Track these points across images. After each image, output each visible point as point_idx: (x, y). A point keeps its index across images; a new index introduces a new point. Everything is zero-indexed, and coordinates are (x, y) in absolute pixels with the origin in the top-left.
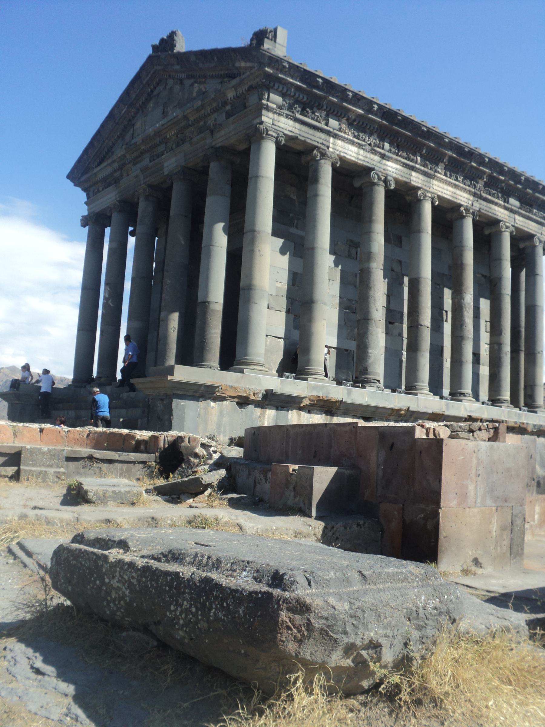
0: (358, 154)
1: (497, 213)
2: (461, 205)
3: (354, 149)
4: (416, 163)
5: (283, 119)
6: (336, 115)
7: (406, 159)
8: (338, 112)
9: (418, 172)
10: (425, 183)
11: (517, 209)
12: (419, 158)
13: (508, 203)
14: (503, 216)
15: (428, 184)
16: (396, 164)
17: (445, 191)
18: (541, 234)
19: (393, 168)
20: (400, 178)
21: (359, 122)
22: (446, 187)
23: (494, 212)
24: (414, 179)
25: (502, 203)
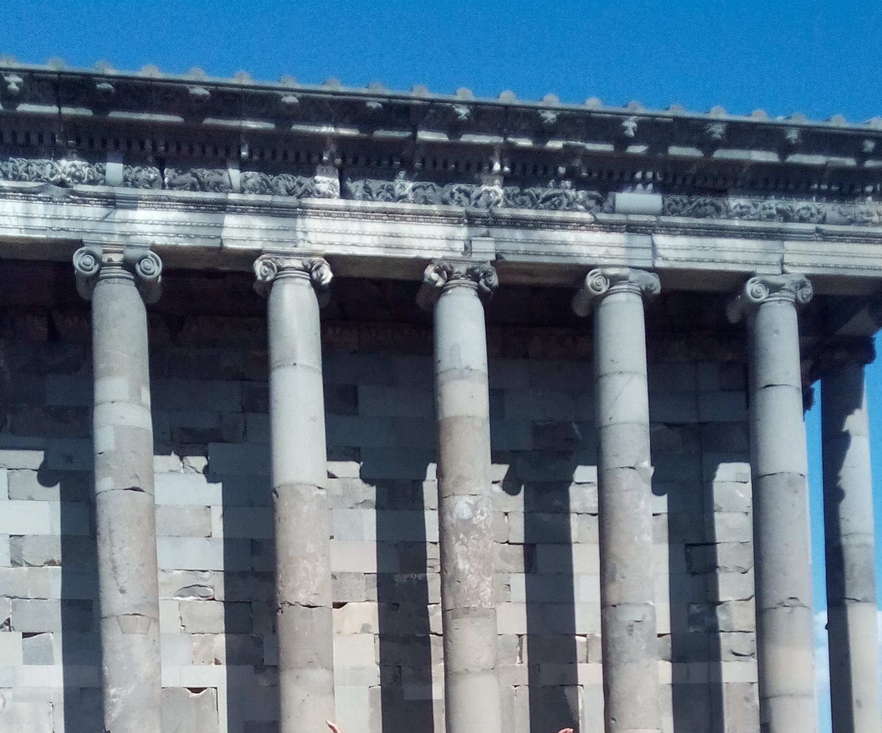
0: (28, 217)
1: (576, 249)
7: (193, 188)
9: (242, 212)
10: (274, 236)
11: (653, 219)
13: (613, 210)
14: (602, 251)
15: (286, 236)
16: (163, 207)
17: (355, 239)
18: (782, 263)
19: (156, 223)
20: (184, 243)
22: (354, 226)
23: (562, 249)
24: (236, 234)
25: (587, 216)
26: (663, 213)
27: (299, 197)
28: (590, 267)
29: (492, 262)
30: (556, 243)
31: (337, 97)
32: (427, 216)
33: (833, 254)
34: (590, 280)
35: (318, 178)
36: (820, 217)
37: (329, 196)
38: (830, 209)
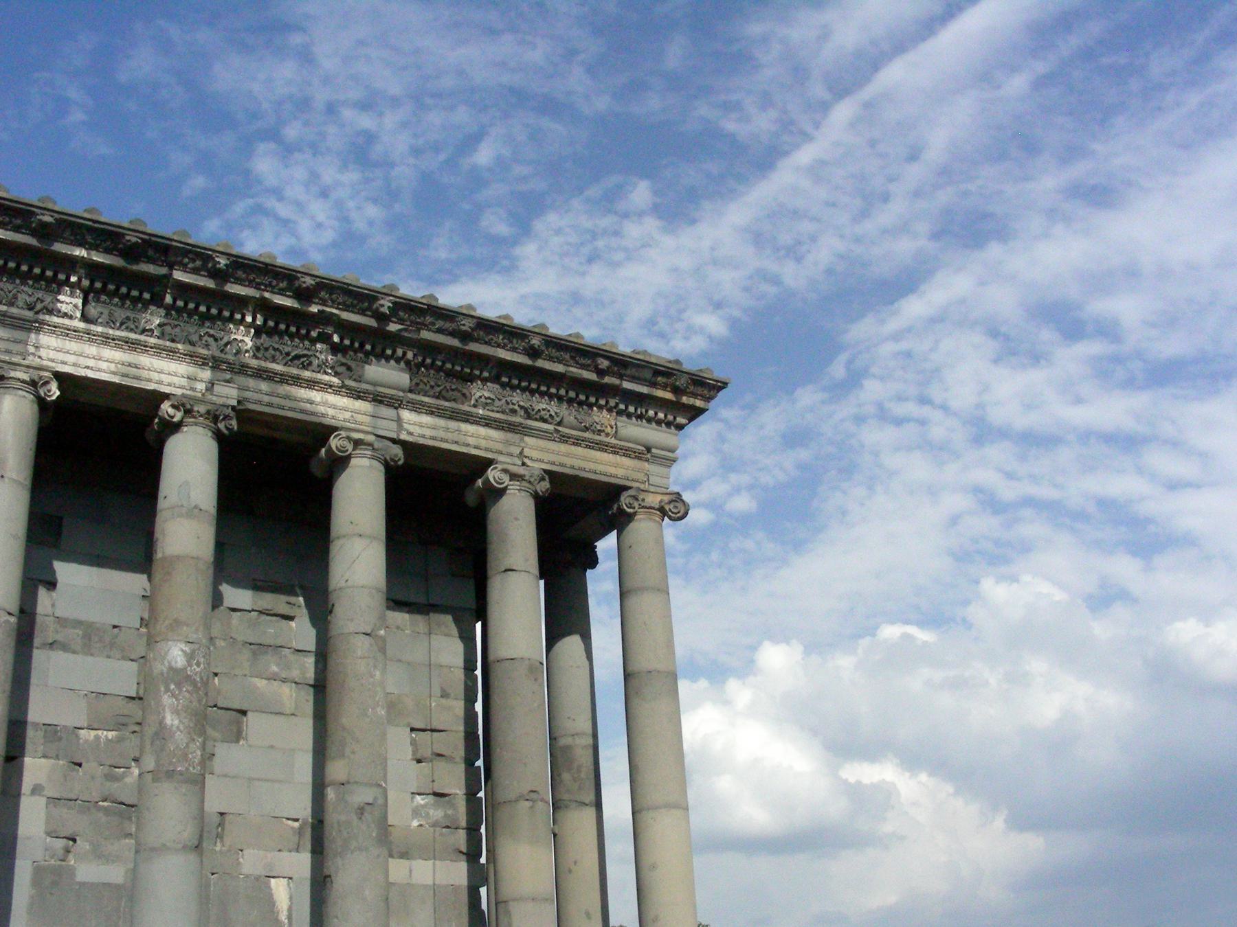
1: (321, 409)
2: (167, 396)
11: (401, 394)
14: (347, 415)
15: (15, 348)
17: (91, 363)
22: (92, 350)
25: (336, 380)
26: (411, 391)
27: (37, 313)
28: (335, 429)
29: (233, 408)
30: (301, 400)
31: (96, 225)
32: (172, 354)
33: (568, 455)
34: (334, 443)
35: (61, 297)
36: (558, 419)
37: (65, 315)
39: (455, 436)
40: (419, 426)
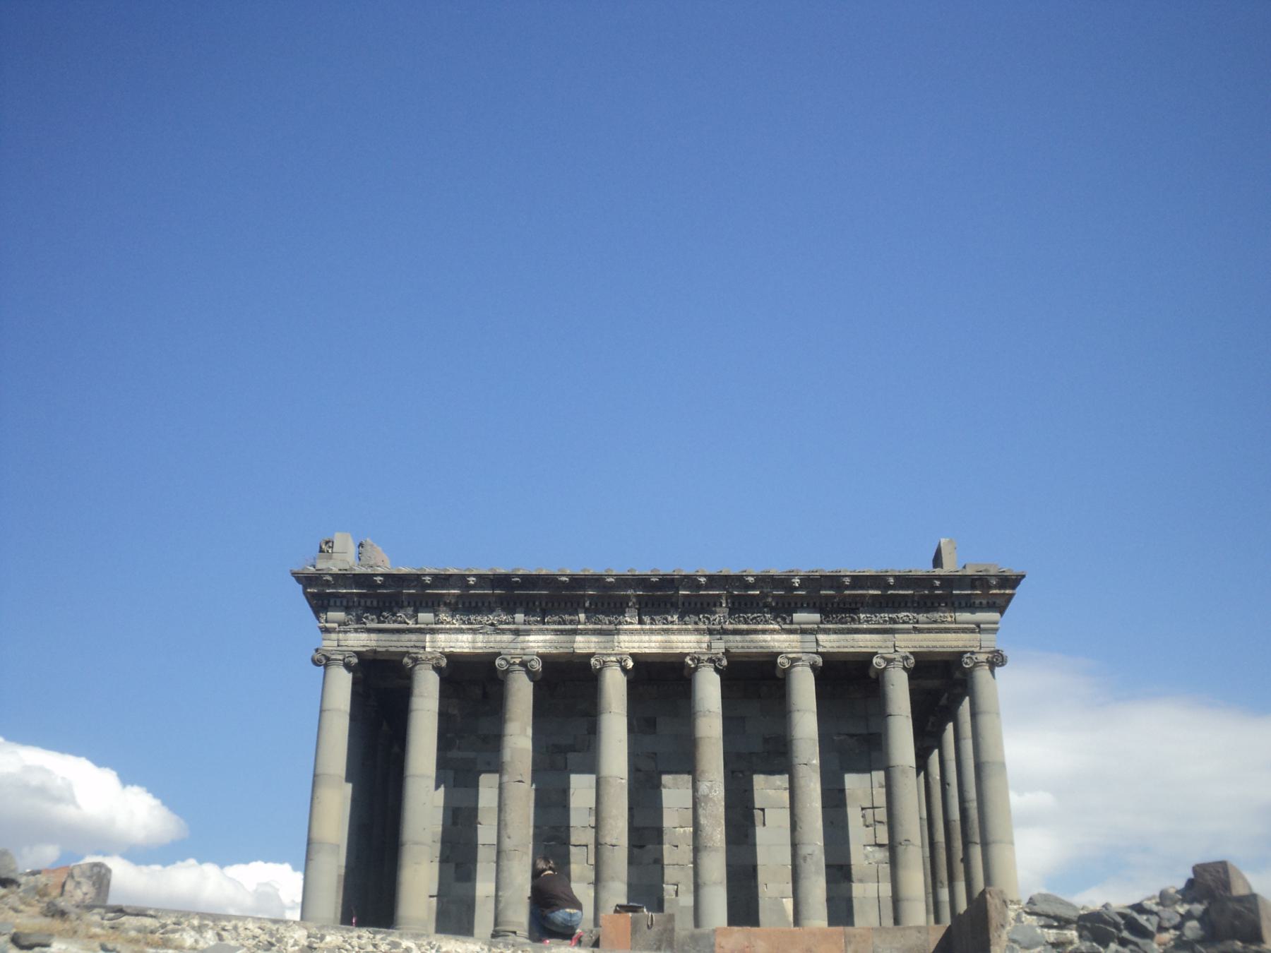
2: (688, 654)
3: (467, 637)
4: (579, 623)
5: (352, 635)
6: (427, 606)
7: (559, 623)
8: (433, 604)
10: (602, 645)
12: (582, 616)
13: (792, 622)
19: (540, 641)
20: (555, 651)
21: (464, 604)
22: (646, 638)
24: (581, 645)
25: (777, 627)
32: (687, 632)
38: (922, 617)
39: (851, 643)
40: (831, 642)
